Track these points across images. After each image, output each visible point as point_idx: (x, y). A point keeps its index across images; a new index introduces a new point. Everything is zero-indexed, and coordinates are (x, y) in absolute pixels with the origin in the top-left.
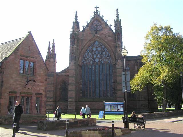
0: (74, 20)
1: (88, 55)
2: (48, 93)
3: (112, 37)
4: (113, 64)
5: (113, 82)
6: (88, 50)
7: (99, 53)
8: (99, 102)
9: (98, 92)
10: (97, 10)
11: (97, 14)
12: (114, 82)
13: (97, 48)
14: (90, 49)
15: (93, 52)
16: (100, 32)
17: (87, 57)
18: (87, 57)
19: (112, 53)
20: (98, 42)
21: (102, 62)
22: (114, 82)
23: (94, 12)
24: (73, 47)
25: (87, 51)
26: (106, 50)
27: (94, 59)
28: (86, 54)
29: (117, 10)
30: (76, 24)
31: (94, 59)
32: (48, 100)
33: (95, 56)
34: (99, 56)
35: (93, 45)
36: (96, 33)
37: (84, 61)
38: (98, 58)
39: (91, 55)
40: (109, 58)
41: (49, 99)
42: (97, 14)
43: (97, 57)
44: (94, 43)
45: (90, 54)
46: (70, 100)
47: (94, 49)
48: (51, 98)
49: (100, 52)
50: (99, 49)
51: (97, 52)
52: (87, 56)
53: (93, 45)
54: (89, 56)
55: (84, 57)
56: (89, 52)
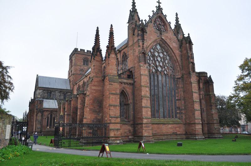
0: (130, 7)
1: (150, 61)
2: (112, 108)
3: (177, 45)
4: (177, 77)
5: (177, 100)
7: (161, 61)
8: (167, 125)
9: (163, 111)
10: (159, 6)
11: (159, 9)
12: (179, 100)
16: (165, 34)
17: (149, 62)
19: (177, 64)
20: (160, 46)
21: (165, 72)
22: (179, 100)
23: (156, 7)
24: (143, 44)
29: (177, 14)
30: (134, 13)
31: (157, 67)
32: (113, 121)
34: (161, 64)
36: (161, 34)
41: (115, 119)
42: (159, 9)
45: (152, 59)
46: (145, 121)
48: (117, 118)
51: (159, 59)
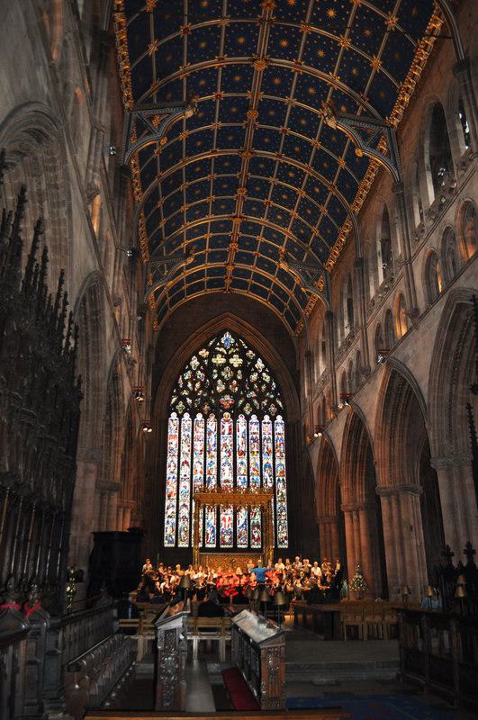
6: (195, 362)
7: (234, 377)
13: (231, 356)
14: (200, 359)
15: (215, 371)
18: (188, 389)
25: (190, 368)
26: (260, 364)
27: (218, 396)
28: (188, 375)
33: (220, 388)
35: (214, 345)
37: (176, 403)
38: (230, 393)
39: (203, 384)
40: (272, 396)
43: (227, 391)
44: (220, 341)
47: (219, 360)
49: (239, 372)
50: (236, 361)
52: (190, 385)
53: (214, 345)
54: (198, 385)
55: (177, 385)
56: (198, 368)
